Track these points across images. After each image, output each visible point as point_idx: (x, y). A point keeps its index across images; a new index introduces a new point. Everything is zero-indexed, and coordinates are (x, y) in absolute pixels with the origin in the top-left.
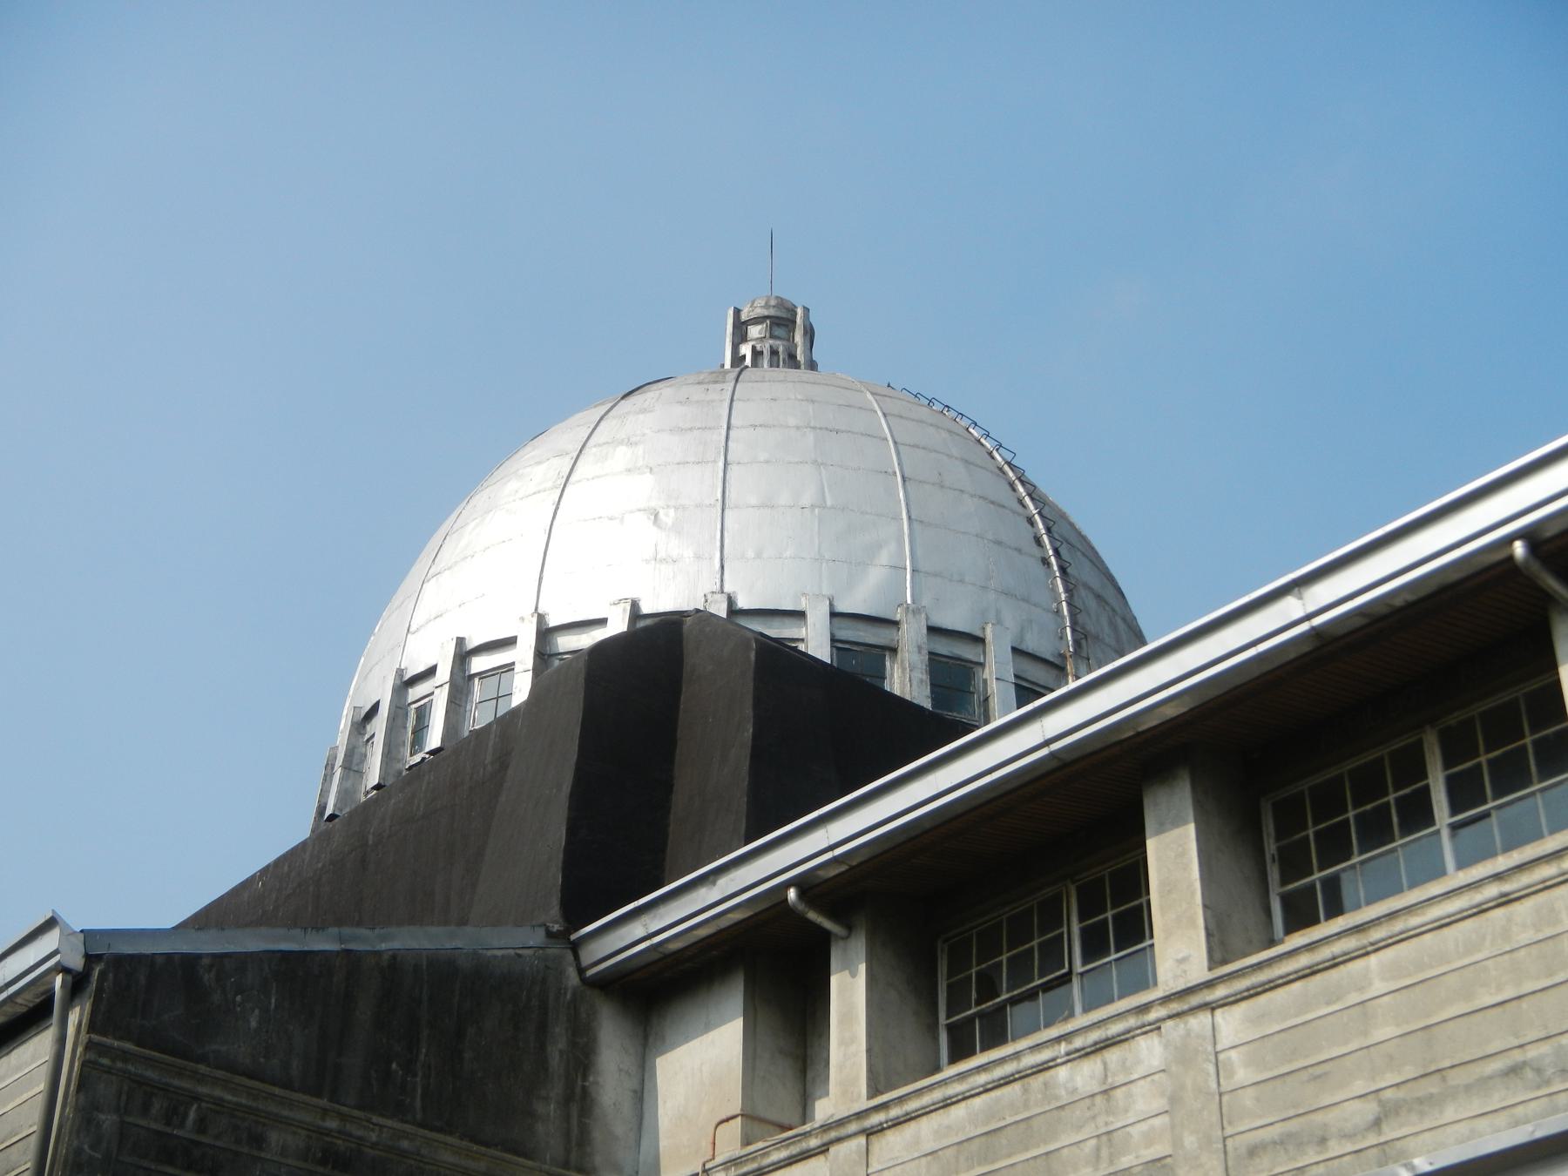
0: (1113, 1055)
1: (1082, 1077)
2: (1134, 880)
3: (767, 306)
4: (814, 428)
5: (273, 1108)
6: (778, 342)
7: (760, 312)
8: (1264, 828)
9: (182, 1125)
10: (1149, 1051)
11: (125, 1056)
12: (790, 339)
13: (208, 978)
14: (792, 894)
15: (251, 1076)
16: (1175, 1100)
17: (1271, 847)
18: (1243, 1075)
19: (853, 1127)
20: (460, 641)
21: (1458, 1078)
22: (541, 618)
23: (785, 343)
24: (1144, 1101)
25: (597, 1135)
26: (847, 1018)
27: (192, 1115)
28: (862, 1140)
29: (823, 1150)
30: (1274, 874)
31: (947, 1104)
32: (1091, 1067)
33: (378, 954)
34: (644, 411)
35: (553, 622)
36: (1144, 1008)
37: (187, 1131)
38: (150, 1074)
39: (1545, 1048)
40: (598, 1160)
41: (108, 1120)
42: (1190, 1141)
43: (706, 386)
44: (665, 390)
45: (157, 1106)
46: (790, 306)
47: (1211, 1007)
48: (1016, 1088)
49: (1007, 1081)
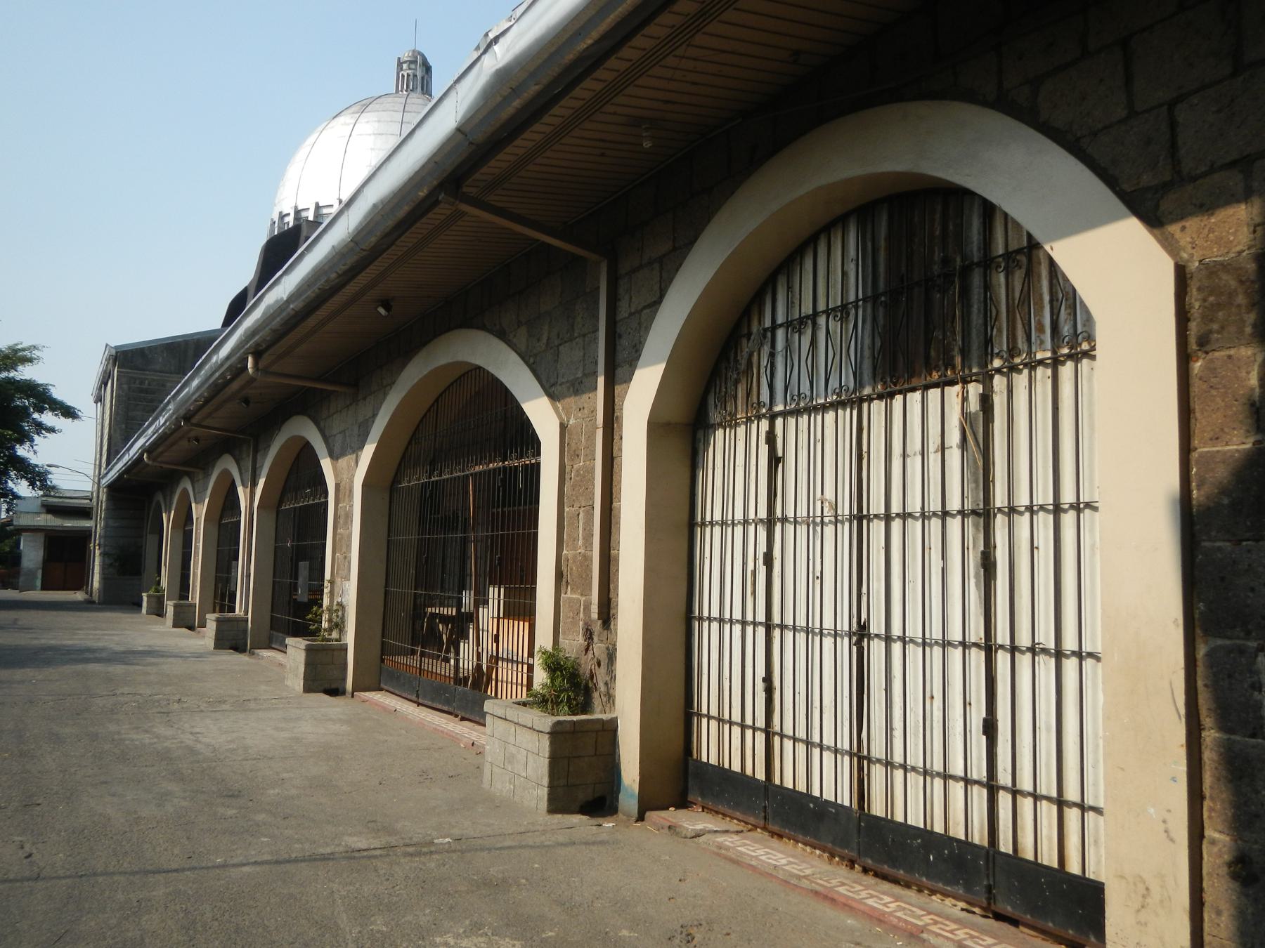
3: (408, 56)
4: (374, 134)
5: (166, 378)
6: (410, 71)
7: (406, 59)
11: (128, 373)
12: (416, 69)
15: (161, 372)
20: (281, 213)
22: (296, 207)
23: (413, 71)
27: (147, 382)
33: (193, 339)
34: (332, 127)
35: (300, 208)
37: (146, 386)
38: (135, 375)
41: (125, 386)
43: (352, 115)
44: (341, 119)
45: (137, 382)
46: (416, 54)
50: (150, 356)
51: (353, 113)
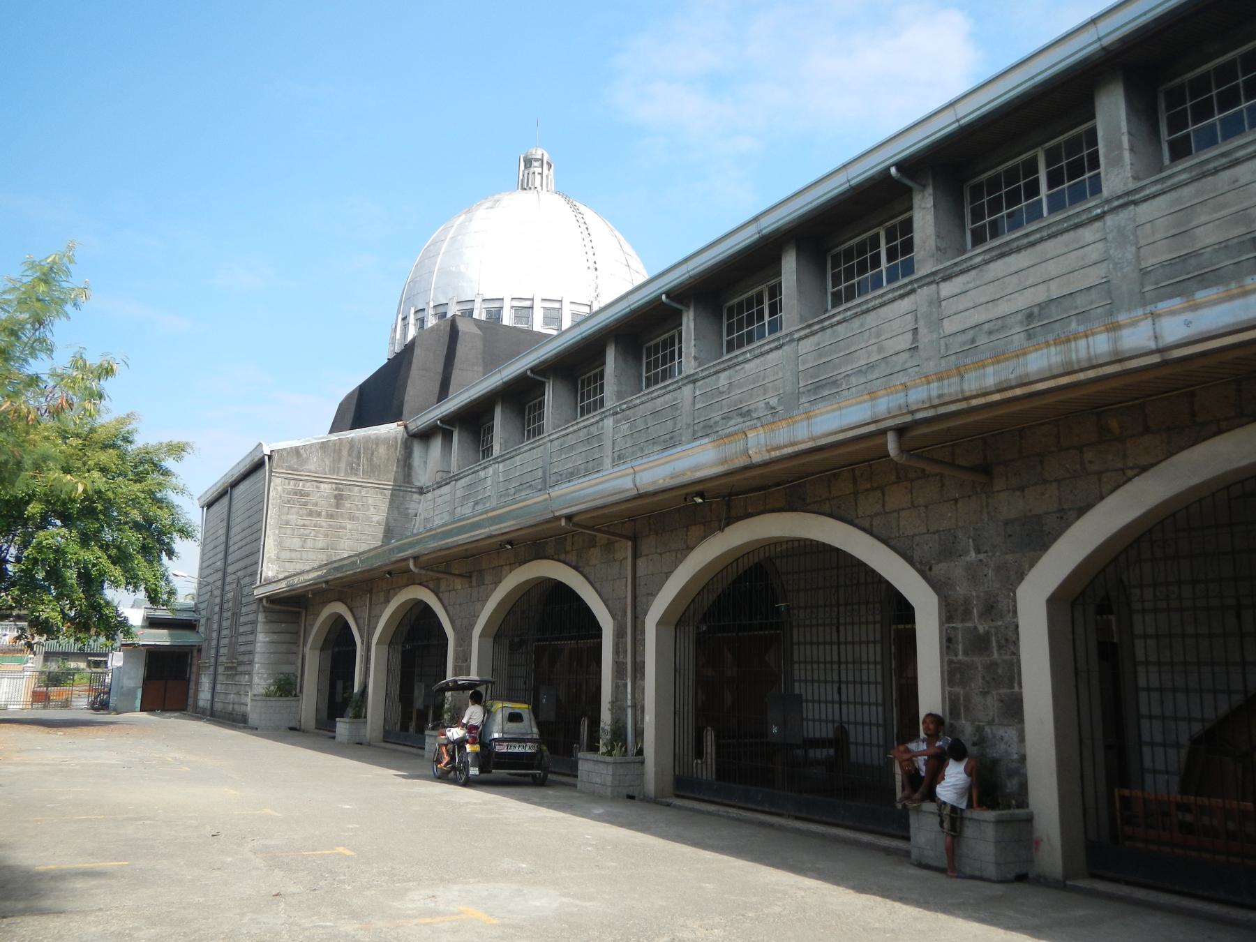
0: (486, 470)
1: (482, 474)
2: (908, 226)
8: (965, 200)
9: (298, 486)
10: (490, 471)
13: (302, 451)
14: (438, 422)
16: (492, 482)
17: (526, 418)
18: (501, 479)
19: (453, 479)
21: (525, 486)
24: (489, 482)
25: (413, 474)
26: (454, 450)
28: (454, 482)
29: (449, 483)
30: (526, 426)
31: (465, 476)
32: (484, 472)
36: (489, 461)
39: (533, 482)
40: (414, 480)
42: (493, 492)
47: (499, 462)
48: (474, 475)
49: (473, 473)
50: (305, 456)
51: (487, 208)
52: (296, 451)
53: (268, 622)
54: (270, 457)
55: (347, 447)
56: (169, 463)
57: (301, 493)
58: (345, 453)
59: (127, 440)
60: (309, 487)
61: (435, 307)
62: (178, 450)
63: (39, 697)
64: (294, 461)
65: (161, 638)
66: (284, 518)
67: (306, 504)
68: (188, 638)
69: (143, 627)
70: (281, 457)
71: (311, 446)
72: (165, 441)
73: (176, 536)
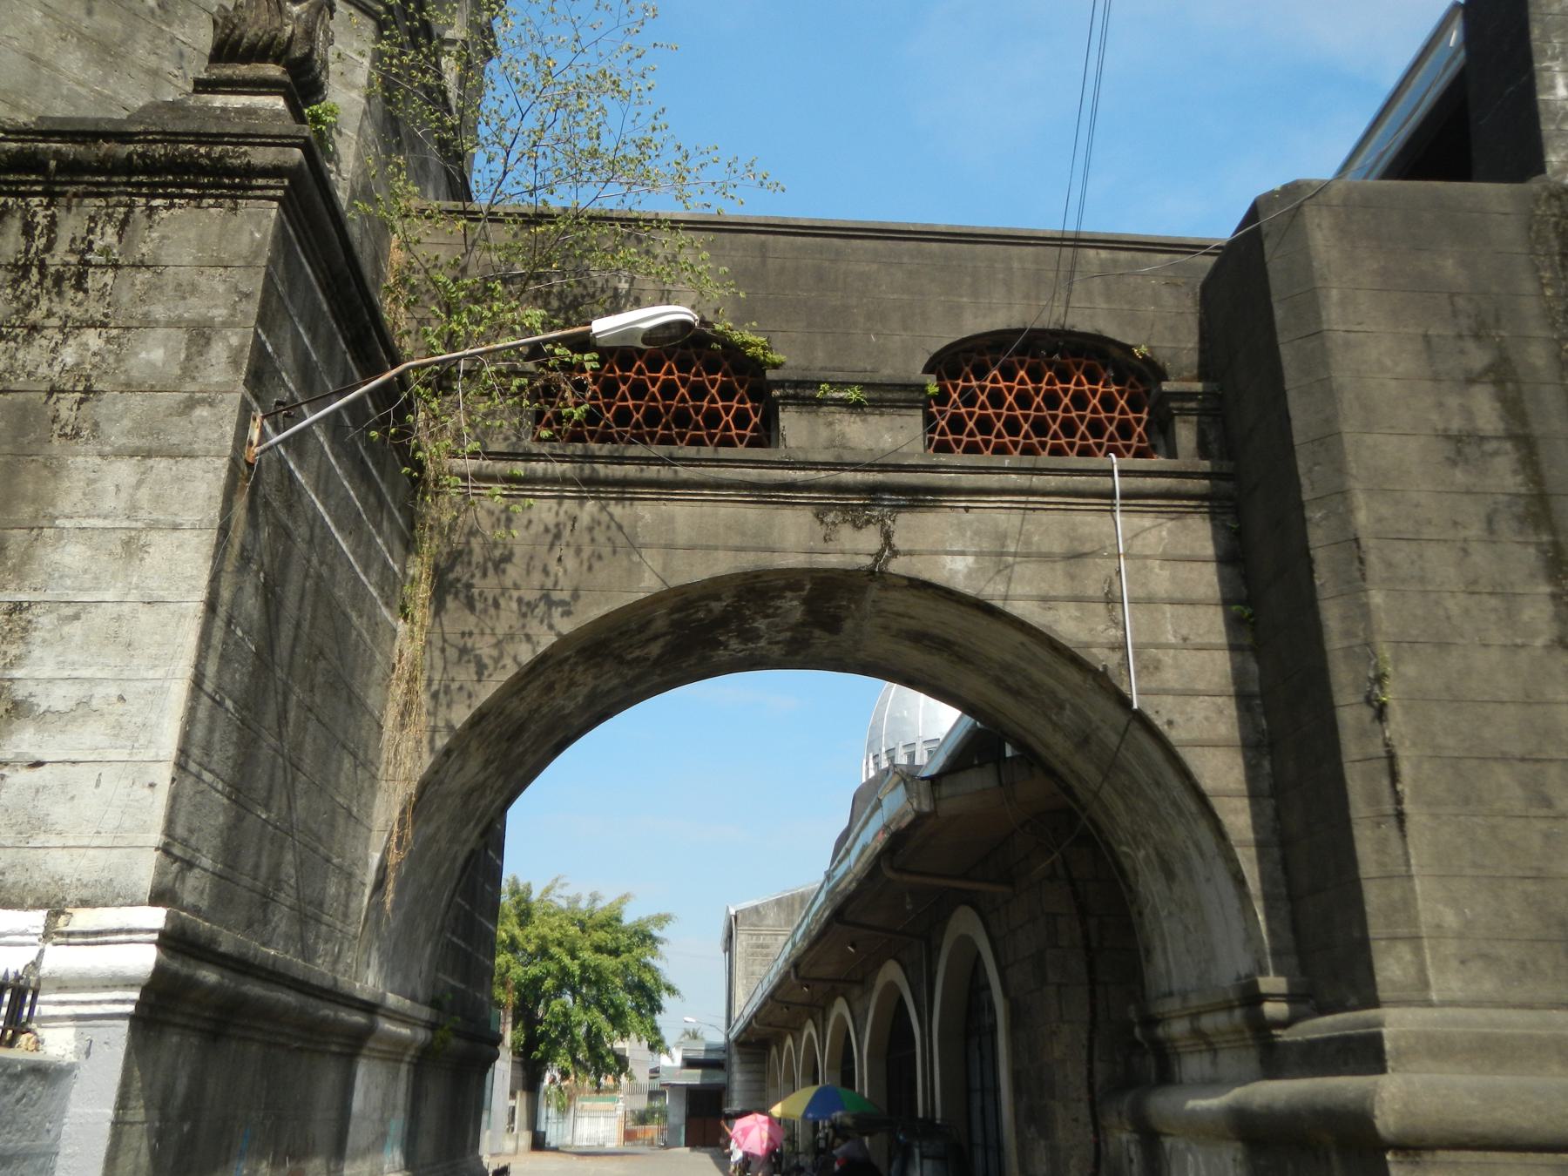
52: (756, 909)
53: (743, 1062)
54: (736, 917)
55: (798, 899)
56: (656, 932)
57: (762, 946)
58: (797, 906)
59: (618, 920)
60: (768, 940)
61: (887, 752)
62: (663, 919)
63: (629, 1136)
64: (754, 919)
65: (694, 1077)
66: (750, 969)
67: (767, 955)
68: (718, 1078)
69: (682, 1068)
70: (743, 917)
71: (767, 904)
72: (654, 913)
73: (665, 995)
